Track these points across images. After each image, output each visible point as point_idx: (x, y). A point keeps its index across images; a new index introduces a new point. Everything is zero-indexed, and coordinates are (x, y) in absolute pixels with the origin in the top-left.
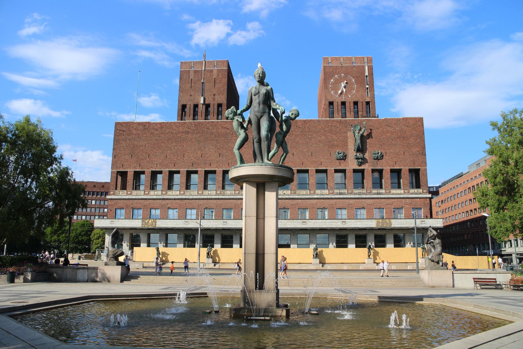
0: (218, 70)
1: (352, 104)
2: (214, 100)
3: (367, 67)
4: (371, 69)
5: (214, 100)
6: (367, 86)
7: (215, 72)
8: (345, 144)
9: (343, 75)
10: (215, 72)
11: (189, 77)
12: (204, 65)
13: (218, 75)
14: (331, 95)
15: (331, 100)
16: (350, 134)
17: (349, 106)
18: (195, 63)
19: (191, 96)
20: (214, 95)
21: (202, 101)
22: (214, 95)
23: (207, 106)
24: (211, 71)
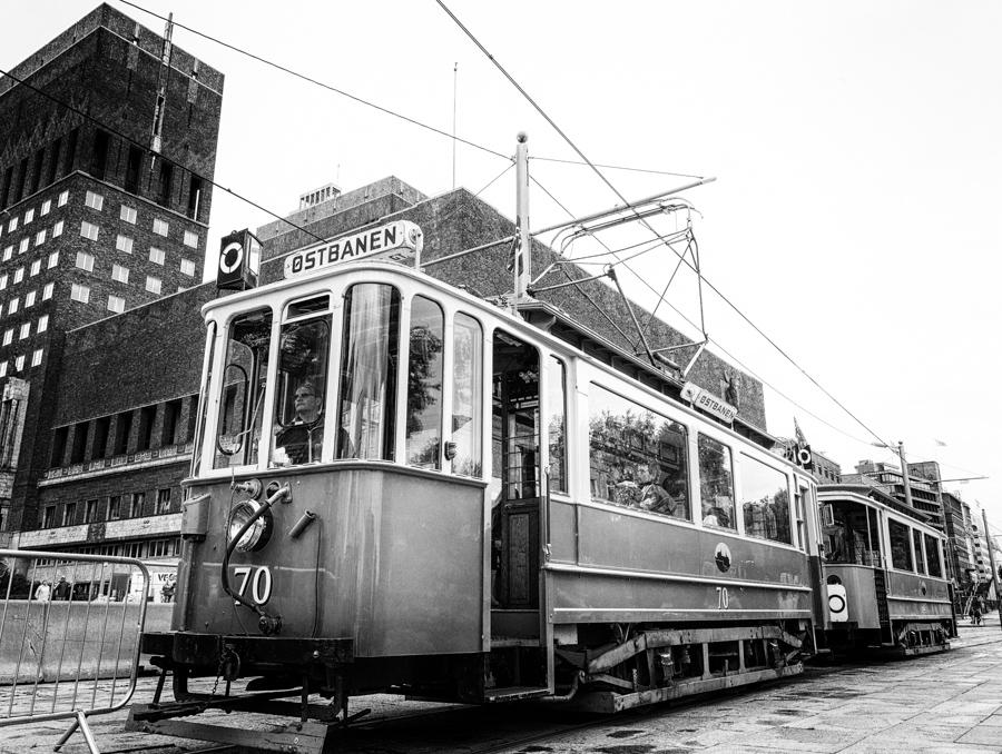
0: (200, 87)
11: (125, 59)
13: (199, 98)
18: (146, 33)
19: (125, 116)
20: (186, 147)
24: (185, 81)
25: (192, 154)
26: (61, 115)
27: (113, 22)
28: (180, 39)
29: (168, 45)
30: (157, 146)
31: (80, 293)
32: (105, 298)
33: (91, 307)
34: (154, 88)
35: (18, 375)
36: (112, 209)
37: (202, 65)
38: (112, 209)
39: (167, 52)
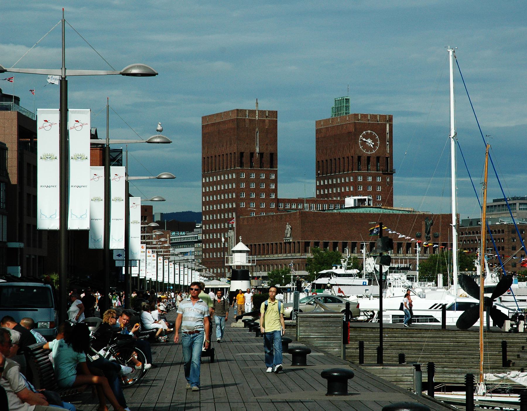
1: (375, 159)
2: (267, 149)
3: (388, 125)
4: (391, 126)
5: (267, 149)
6: (388, 143)
7: (267, 122)
8: (420, 230)
9: (369, 131)
10: (267, 122)
11: (245, 125)
12: (257, 114)
13: (269, 126)
14: (360, 150)
15: (360, 155)
16: (423, 223)
17: (373, 160)
19: (247, 144)
21: (258, 150)
22: (267, 144)
23: (261, 154)
25: (269, 146)
26: (231, 144)
27: (240, 114)
28: (262, 107)
29: (257, 112)
30: (258, 150)
31: (243, 205)
32: (249, 204)
33: (246, 208)
34: (254, 130)
35: (231, 229)
36: (248, 176)
37: (269, 111)
38: (248, 176)
39: (257, 114)
